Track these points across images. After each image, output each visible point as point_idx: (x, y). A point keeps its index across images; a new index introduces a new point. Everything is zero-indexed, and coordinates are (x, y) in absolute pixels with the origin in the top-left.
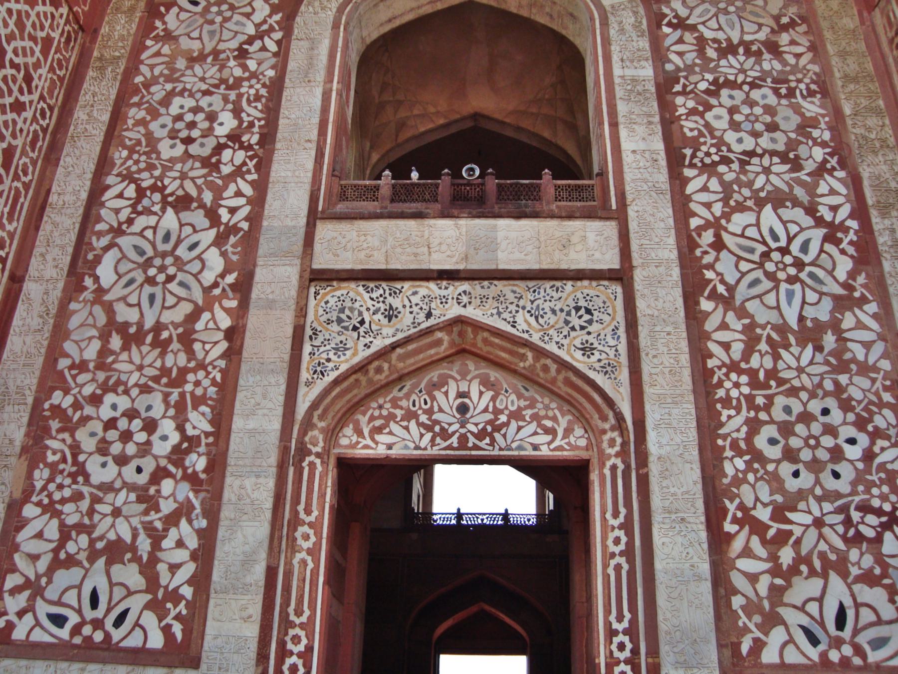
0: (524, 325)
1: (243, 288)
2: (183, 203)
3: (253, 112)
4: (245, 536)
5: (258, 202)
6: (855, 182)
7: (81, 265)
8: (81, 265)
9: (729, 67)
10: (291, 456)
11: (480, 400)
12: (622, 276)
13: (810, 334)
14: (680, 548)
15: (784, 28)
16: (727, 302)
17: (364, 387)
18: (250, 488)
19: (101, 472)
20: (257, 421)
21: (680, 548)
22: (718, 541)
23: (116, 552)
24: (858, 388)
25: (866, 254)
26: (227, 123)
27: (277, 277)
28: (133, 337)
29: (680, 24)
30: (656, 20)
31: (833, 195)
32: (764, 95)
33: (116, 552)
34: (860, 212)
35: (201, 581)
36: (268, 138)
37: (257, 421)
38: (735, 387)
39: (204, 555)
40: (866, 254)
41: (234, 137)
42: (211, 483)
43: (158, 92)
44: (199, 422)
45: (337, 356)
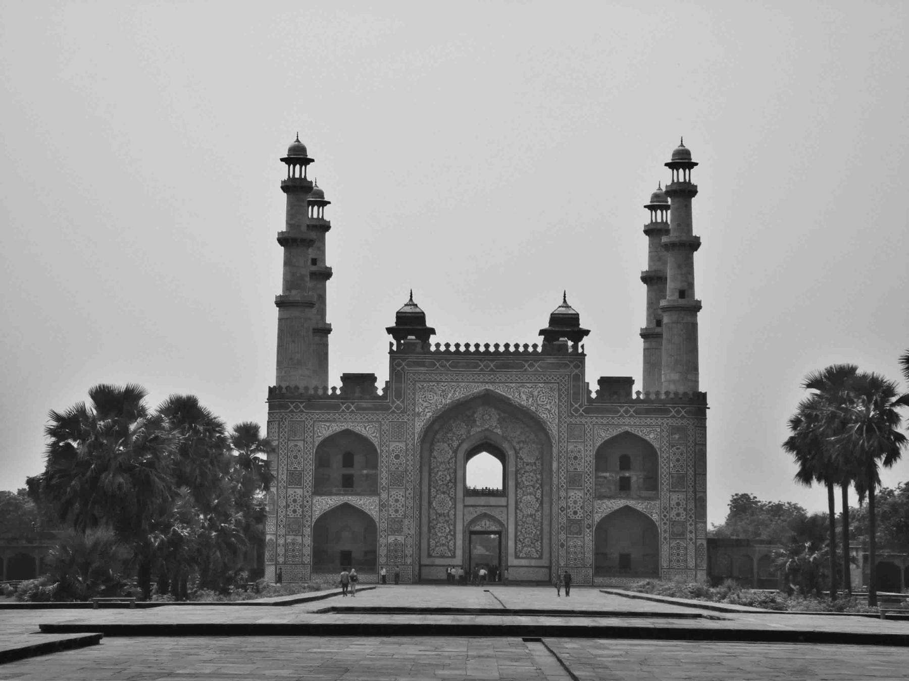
0: (493, 514)
1: (455, 508)
2: (444, 493)
3: (452, 475)
4: (459, 543)
5: (455, 493)
6: (542, 492)
7: (430, 503)
8: (430, 503)
9: (527, 468)
10: (464, 532)
11: (488, 523)
12: (507, 506)
13: (531, 515)
14: (511, 544)
15: (537, 459)
16: (521, 511)
17: (473, 522)
18: (459, 536)
19: (440, 534)
20: (459, 528)
21: (511, 544)
22: (516, 543)
23: (443, 545)
24: (536, 523)
25: (541, 504)
26: (448, 478)
27: (460, 506)
28: (440, 516)
29: (521, 459)
30: (517, 457)
31: (539, 494)
32: (532, 474)
33: (443, 545)
34: (542, 497)
35: (455, 548)
36: (455, 480)
37: (459, 528)
38: (520, 523)
39: (455, 544)
40: (541, 504)
41: (450, 480)
42: (454, 535)
43: (436, 470)
44: (451, 528)
45: (469, 518)
